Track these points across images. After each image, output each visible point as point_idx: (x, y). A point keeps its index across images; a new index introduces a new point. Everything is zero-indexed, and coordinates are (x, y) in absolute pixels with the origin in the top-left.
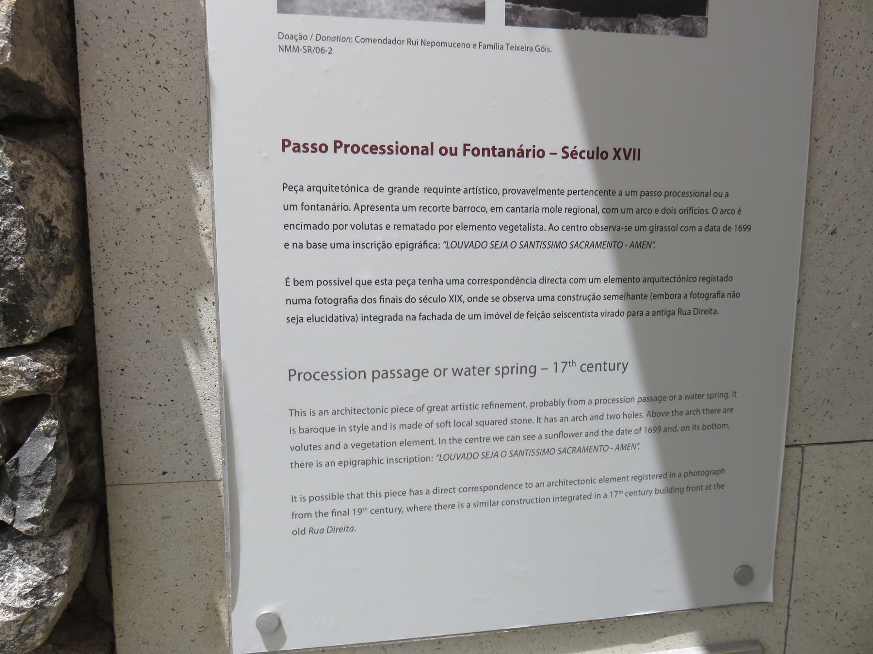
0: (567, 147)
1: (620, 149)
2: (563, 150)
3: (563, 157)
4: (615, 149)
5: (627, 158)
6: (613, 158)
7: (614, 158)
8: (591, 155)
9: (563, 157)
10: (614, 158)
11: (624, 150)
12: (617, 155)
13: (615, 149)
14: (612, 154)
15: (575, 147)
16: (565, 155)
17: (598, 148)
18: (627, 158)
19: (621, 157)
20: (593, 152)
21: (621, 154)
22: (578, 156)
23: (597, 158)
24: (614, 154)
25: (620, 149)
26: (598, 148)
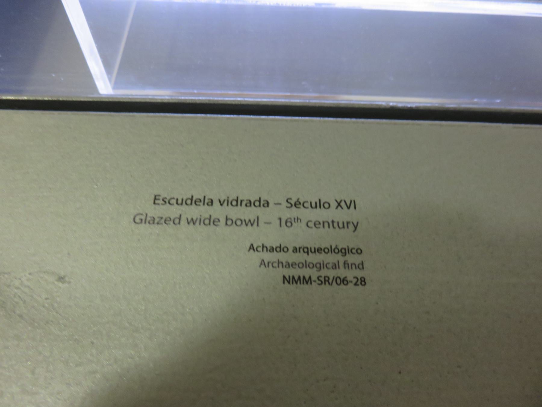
0: (291, 199)
1: (341, 201)
2: (287, 201)
3: (287, 207)
4: (336, 201)
5: (349, 208)
6: (335, 207)
7: (337, 208)
8: (314, 205)
9: (287, 207)
10: (337, 208)
11: (345, 201)
12: (339, 204)
13: (336, 201)
14: (334, 204)
15: (298, 199)
16: (289, 205)
17: (320, 200)
18: (349, 208)
19: (343, 207)
20: (316, 203)
21: (343, 204)
22: (301, 206)
23: (320, 207)
24: (337, 204)
25: (341, 201)
26: (320, 200)
